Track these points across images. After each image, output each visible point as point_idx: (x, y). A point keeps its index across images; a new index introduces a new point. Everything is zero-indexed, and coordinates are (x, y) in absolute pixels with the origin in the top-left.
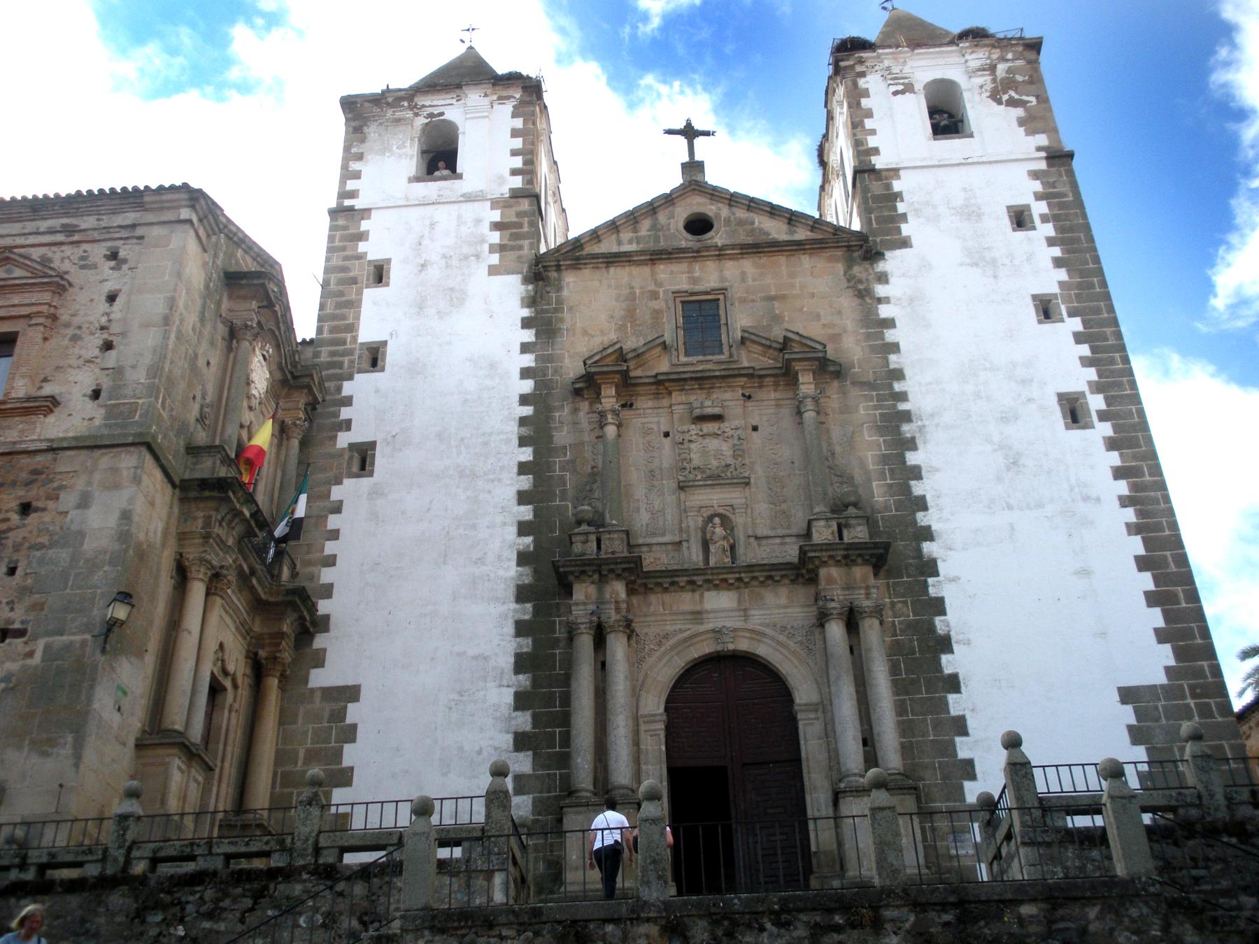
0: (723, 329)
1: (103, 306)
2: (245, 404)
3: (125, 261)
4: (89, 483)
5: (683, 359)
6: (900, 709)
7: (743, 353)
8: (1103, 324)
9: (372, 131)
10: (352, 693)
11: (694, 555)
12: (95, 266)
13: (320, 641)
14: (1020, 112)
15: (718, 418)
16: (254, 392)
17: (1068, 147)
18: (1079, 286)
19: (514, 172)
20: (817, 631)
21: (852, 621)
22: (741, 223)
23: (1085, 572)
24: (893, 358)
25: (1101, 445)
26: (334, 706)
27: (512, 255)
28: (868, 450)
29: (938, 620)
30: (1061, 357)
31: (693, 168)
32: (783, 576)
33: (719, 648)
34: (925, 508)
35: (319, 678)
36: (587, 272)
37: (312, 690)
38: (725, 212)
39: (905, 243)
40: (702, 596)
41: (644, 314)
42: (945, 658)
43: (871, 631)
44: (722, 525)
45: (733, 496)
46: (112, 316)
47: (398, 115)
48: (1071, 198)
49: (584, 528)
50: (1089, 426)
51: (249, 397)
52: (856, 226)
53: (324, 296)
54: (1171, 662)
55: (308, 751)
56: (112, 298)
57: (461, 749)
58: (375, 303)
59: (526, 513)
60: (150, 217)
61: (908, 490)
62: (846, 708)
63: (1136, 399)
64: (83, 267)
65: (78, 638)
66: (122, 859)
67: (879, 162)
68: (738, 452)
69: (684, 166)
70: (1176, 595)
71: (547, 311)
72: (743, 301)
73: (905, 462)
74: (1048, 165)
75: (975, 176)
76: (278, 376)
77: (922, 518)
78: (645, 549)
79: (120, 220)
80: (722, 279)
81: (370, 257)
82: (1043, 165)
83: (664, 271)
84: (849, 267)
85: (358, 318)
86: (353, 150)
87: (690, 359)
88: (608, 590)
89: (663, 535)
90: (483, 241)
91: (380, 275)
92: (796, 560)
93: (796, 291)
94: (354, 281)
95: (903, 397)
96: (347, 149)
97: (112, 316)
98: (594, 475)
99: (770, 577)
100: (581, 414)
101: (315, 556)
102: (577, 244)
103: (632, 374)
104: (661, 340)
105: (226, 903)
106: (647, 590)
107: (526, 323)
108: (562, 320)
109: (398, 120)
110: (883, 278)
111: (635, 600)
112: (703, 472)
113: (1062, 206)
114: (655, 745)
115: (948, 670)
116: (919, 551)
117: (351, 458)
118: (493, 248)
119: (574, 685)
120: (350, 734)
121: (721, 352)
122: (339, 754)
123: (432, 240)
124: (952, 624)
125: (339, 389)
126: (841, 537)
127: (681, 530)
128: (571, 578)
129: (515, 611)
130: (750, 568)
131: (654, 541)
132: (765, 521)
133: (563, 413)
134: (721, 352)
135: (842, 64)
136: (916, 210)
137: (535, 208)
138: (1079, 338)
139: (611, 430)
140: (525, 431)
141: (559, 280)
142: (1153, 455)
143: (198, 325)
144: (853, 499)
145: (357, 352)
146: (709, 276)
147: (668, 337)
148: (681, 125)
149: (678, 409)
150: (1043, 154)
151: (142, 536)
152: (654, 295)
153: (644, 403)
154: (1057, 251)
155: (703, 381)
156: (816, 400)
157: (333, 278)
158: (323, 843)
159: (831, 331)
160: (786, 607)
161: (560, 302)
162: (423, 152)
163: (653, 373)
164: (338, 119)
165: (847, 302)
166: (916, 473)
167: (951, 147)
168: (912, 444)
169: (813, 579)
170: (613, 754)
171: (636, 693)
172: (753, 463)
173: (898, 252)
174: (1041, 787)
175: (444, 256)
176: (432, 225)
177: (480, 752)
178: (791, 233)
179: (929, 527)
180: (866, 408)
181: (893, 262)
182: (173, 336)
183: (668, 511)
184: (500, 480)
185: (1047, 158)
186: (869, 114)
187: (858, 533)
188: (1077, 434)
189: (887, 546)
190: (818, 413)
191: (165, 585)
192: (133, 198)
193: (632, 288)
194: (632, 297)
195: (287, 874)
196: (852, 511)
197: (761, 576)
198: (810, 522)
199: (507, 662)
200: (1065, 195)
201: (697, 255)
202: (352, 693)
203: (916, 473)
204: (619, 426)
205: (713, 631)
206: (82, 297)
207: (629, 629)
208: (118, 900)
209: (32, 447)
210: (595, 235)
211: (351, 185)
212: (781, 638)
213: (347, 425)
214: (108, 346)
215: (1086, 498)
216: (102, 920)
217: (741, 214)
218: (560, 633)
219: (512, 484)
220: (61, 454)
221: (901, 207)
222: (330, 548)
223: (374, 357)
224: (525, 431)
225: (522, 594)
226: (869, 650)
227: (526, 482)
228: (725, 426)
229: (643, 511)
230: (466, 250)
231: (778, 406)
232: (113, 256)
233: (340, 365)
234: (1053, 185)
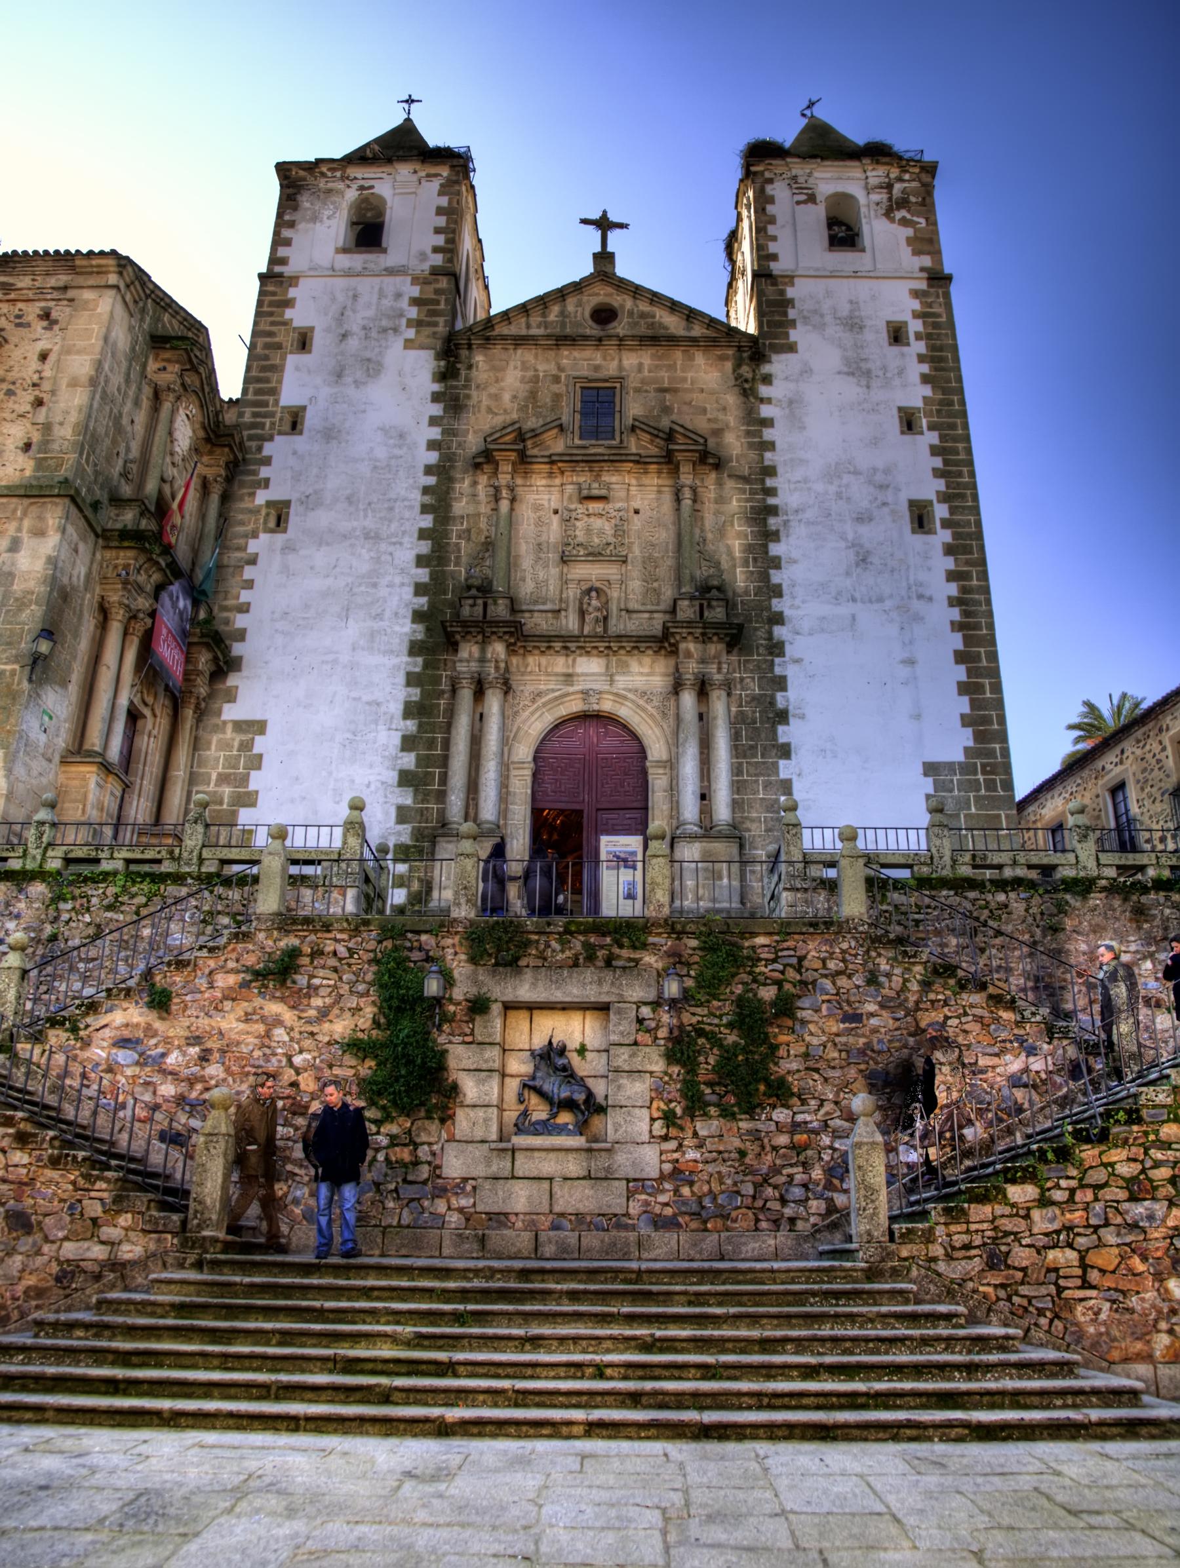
0: (617, 416)
1: (34, 364)
2: (168, 460)
3: (56, 322)
4: (19, 530)
5: (577, 442)
6: (736, 770)
7: (633, 440)
8: (955, 439)
9: (305, 201)
10: (260, 727)
11: (571, 623)
12: (28, 325)
13: (232, 680)
14: (910, 232)
16: (177, 449)
17: (947, 271)
18: (942, 403)
19: (436, 250)
20: (673, 699)
22: (643, 315)
23: (910, 662)
24: (768, 455)
25: (939, 549)
26: (244, 737)
27: (428, 331)
29: (779, 696)
30: (916, 469)
31: (604, 258)
33: (586, 708)
34: (780, 595)
35: (231, 712)
36: (497, 351)
37: (225, 723)
38: (629, 304)
39: (792, 348)
40: (574, 661)
41: (545, 397)
42: (781, 729)
44: (598, 597)
45: (611, 571)
46: (44, 374)
47: (330, 185)
48: (944, 319)
49: (474, 592)
50: (931, 532)
51: (172, 454)
52: (752, 329)
53: (251, 358)
54: (971, 743)
55: (219, 774)
56: (43, 357)
57: (353, 781)
58: (297, 369)
59: (423, 575)
60: (80, 280)
62: (689, 767)
63: (976, 510)
64: (18, 325)
65: (8, 667)
66: (39, 857)
67: (776, 267)
68: (619, 531)
69: (595, 255)
70: (982, 686)
71: (456, 387)
72: (638, 390)
73: (767, 553)
74: (929, 286)
75: (863, 288)
76: (201, 434)
77: (777, 605)
78: (527, 615)
79: (52, 282)
80: (620, 368)
81: (296, 324)
82: (922, 285)
84: (738, 365)
85: (280, 381)
86: (287, 218)
88: (490, 650)
89: (544, 603)
90: (401, 315)
91: (304, 342)
92: (660, 634)
93: (687, 385)
94: (279, 346)
95: (772, 492)
96: (280, 215)
97: (44, 374)
98: (489, 545)
99: (637, 648)
100: (480, 487)
101: (231, 602)
102: (489, 322)
103: (529, 453)
105: (124, 899)
106: (527, 652)
107: (436, 398)
108: (468, 397)
109: (329, 191)
110: (767, 379)
111: (515, 660)
112: (586, 548)
113: (936, 325)
115: (782, 739)
116: (770, 633)
117: (268, 515)
118: (410, 324)
119: (454, 732)
120: (257, 762)
121: (613, 438)
122: (245, 779)
123: (354, 311)
124: (792, 700)
125: (260, 449)
127: (561, 600)
128: (458, 637)
129: (408, 664)
130: (619, 637)
131: (537, 608)
133: (463, 485)
134: (613, 438)
135: (753, 169)
136: (805, 318)
137: (453, 286)
138: (935, 451)
139: (504, 505)
140: (428, 499)
141: (469, 358)
142: (982, 562)
143: (123, 387)
144: (715, 583)
145: (279, 415)
148: (596, 215)
149: (570, 489)
150: (925, 275)
151: (65, 580)
152: (556, 379)
153: (539, 481)
154: (925, 368)
155: (592, 462)
156: (694, 490)
157: (260, 341)
158: (205, 854)
159: (715, 426)
160: (648, 675)
161: (468, 379)
163: (547, 453)
164: (272, 188)
165: (732, 399)
166: (776, 563)
167: (844, 259)
168: (775, 536)
169: (674, 652)
171: (506, 742)
173: (784, 357)
174: (807, 844)
175: (364, 328)
176: (355, 297)
177: (368, 786)
178: (689, 329)
179: (781, 613)
180: (739, 500)
181: (778, 365)
182: (98, 397)
183: (551, 582)
184: (401, 544)
185: (929, 279)
186: (772, 220)
187: (717, 613)
188: (919, 539)
189: (740, 627)
190: (695, 501)
191: (89, 625)
192: (65, 260)
194: (535, 379)
195: (178, 879)
196: (714, 592)
198: (675, 601)
199: (396, 708)
200: (939, 316)
202: (260, 727)
203: (776, 563)
204: (513, 500)
205: (582, 692)
206: (17, 354)
207: (507, 688)
208: (38, 889)
210: (506, 315)
211: (282, 252)
212: (641, 702)
213: (266, 483)
214: (39, 403)
215: (920, 597)
216: (22, 905)
217: (644, 307)
218: (444, 686)
219: (410, 549)
221: (792, 314)
222: (245, 595)
223: (295, 422)
224: (428, 499)
225: (415, 649)
226: (715, 718)
227: (425, 547)
228: (609, 507)
229: (528, 580)
230: (385, 323)
231: (659, 492)
232: (46, 315)
233: (262, 426)
234: (930, 305)
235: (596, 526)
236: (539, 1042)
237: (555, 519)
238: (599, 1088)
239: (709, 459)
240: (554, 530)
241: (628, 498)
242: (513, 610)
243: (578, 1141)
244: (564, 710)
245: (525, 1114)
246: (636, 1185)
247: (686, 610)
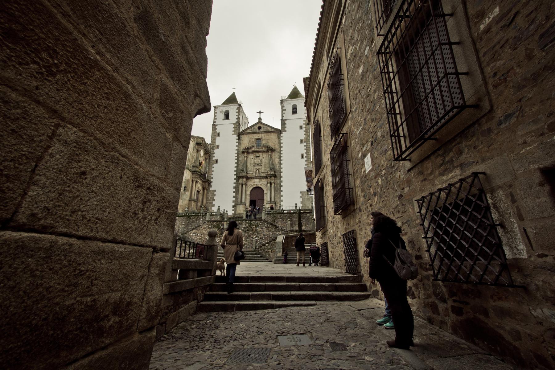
10: (215, 191)
13: (211, 184)
21: (271, 184)
28: (276, 161)
31: (260, 119)
35: (211, 189)
39: (286, 131)
41: (251, 142)
43: (273, 185)
45: (260, 167)
62: (269, 194)
68: (261, 161)
102: (243, 131)
114: (248, 198)
120: (215, 195)
132: (264, 170)
133: (240, 156)
138: (305, 146)
146: (260, 136)
155: (258, 152)
165: (277, 140)
187: (273, 173)
191: (191, 183)
201: (259, 133)
202: (215, 191)
203: (282, 164)
207: (246, 185)
210: (246, 130)
222: (213, 173)
239: (273, 150)
240: (252, 162)
242: (247, 174)
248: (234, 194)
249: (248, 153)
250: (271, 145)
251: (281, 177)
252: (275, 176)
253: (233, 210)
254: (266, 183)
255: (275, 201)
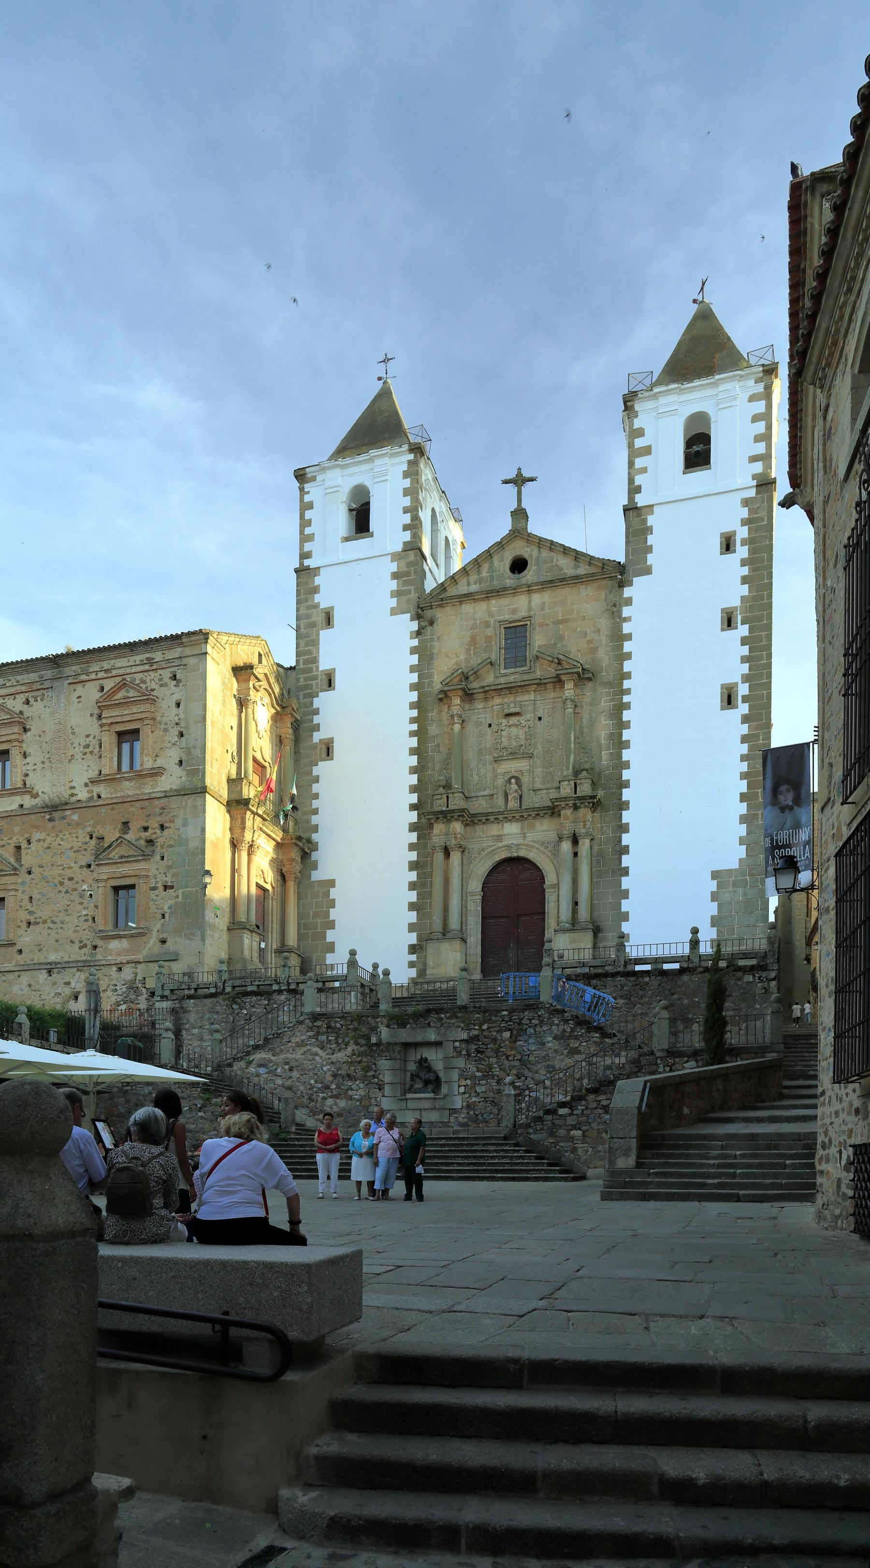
0: (528, 647)
15: (517, 714)
21: (575, 841)
28: (603, 728)
32: (545, 814)
33: (509, 855)
36: (449, 609)
40: (503, 826)
43: (585, 845)
61: (620, 756)
68: (529, 736)
83: (495, 604)
87: (507, 671)
102: (442, 587)
104: (489, 661)
114: (475, 907)
126: (575, 793)
132: (539, 780)
134: (525, 665)
144: (586, 766)
147: (493, 657)
155: (510, 689)
162: (351, 510)
170: (450, 914)
172: (537, 742)
180: (606, 701)
187: (585, 789)
193: (475, 619)
197: (533, 814)
203: (627, 745)
209: (159, 795)
220: (171, 798)
228: (522, 719)
235: (513, 734)
236: (419, 1057)
237: (489, 731)
238: (441, 1075)
241: (535, 710)
243: (432, 1095)
244: (498, 857)
245: (412, 1086)
246: (453, 1111)
247: (566, 790)
248: (413, 896)
249: (468, 696)
250: (576, 649)
251: (625, 806)
252: (595, 804)
253: (411, 965)
254: (552, 836)
255: (592, 921)
